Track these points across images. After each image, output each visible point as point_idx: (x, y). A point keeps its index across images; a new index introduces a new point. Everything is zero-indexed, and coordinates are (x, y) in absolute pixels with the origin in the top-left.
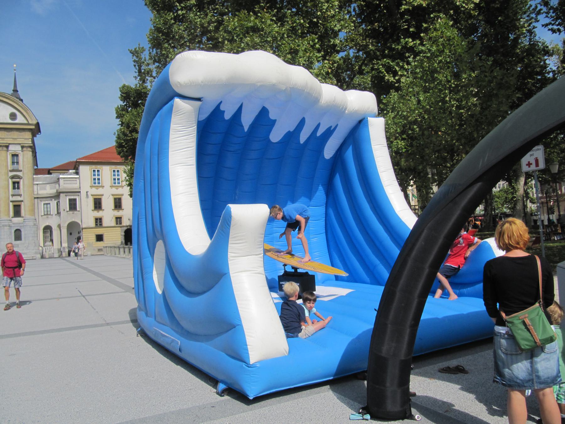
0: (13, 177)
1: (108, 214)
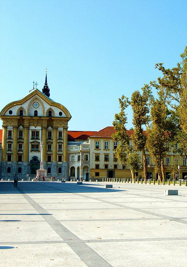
0: (59, 143)
1: (102, 163)
